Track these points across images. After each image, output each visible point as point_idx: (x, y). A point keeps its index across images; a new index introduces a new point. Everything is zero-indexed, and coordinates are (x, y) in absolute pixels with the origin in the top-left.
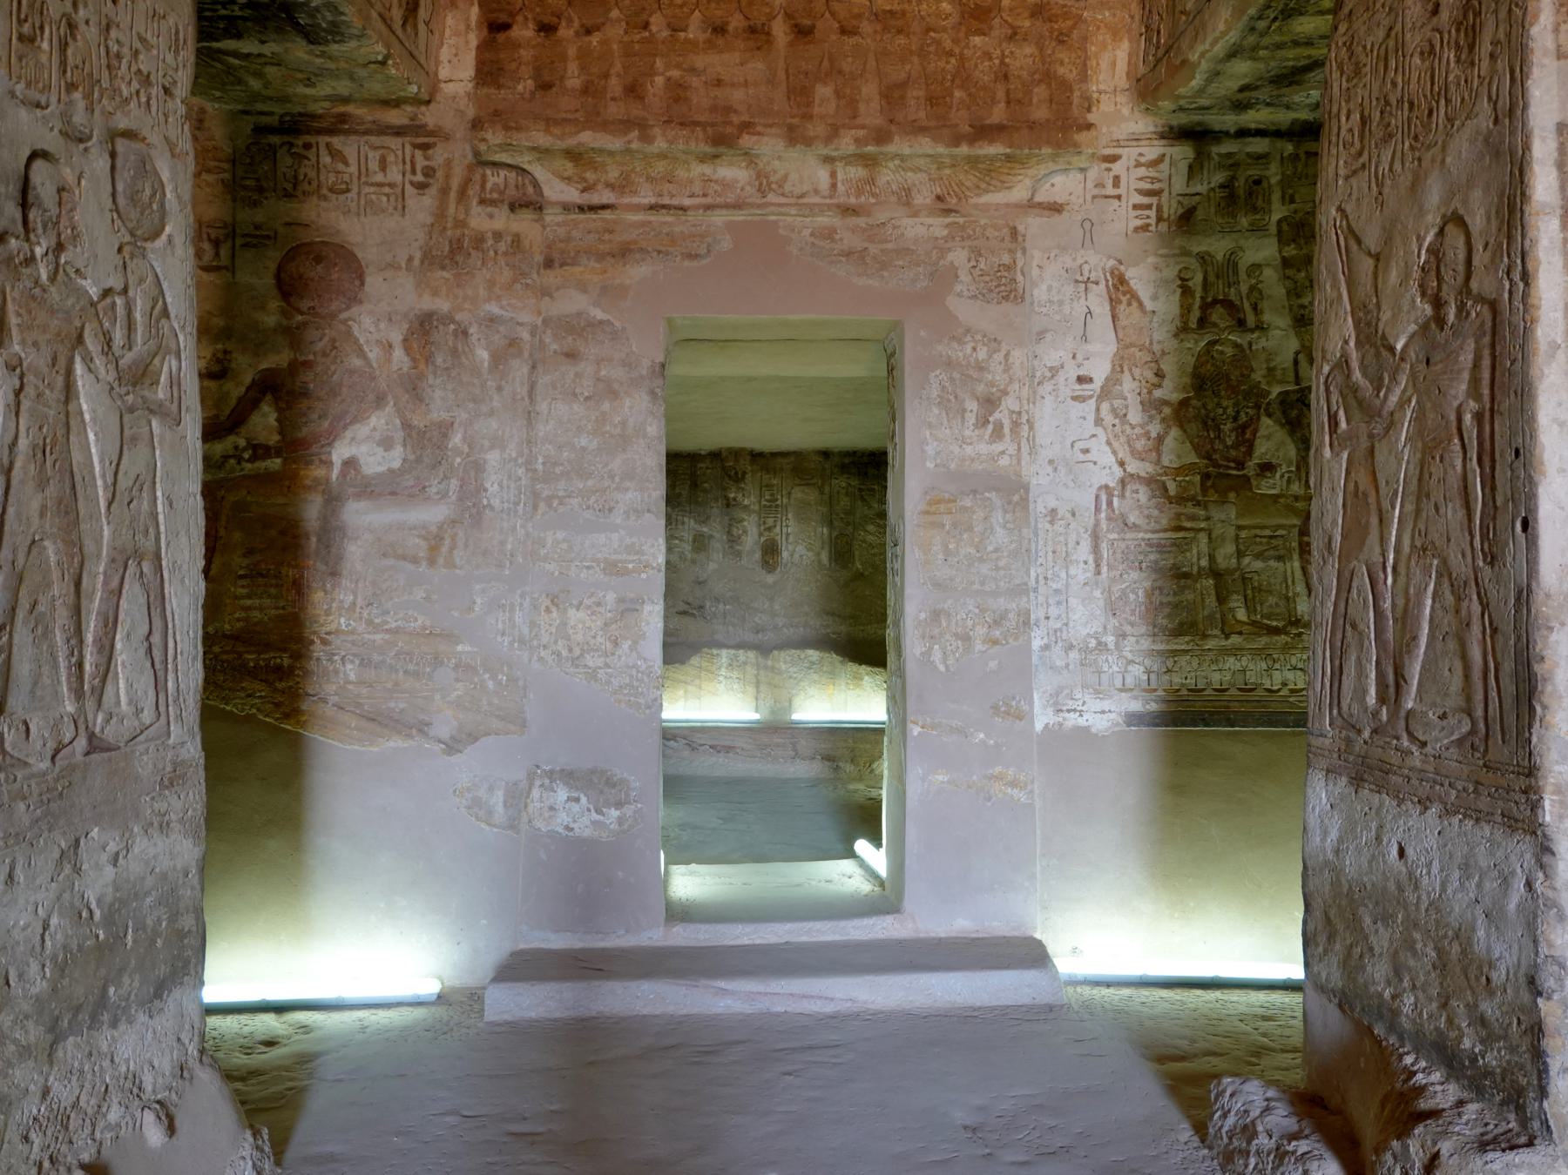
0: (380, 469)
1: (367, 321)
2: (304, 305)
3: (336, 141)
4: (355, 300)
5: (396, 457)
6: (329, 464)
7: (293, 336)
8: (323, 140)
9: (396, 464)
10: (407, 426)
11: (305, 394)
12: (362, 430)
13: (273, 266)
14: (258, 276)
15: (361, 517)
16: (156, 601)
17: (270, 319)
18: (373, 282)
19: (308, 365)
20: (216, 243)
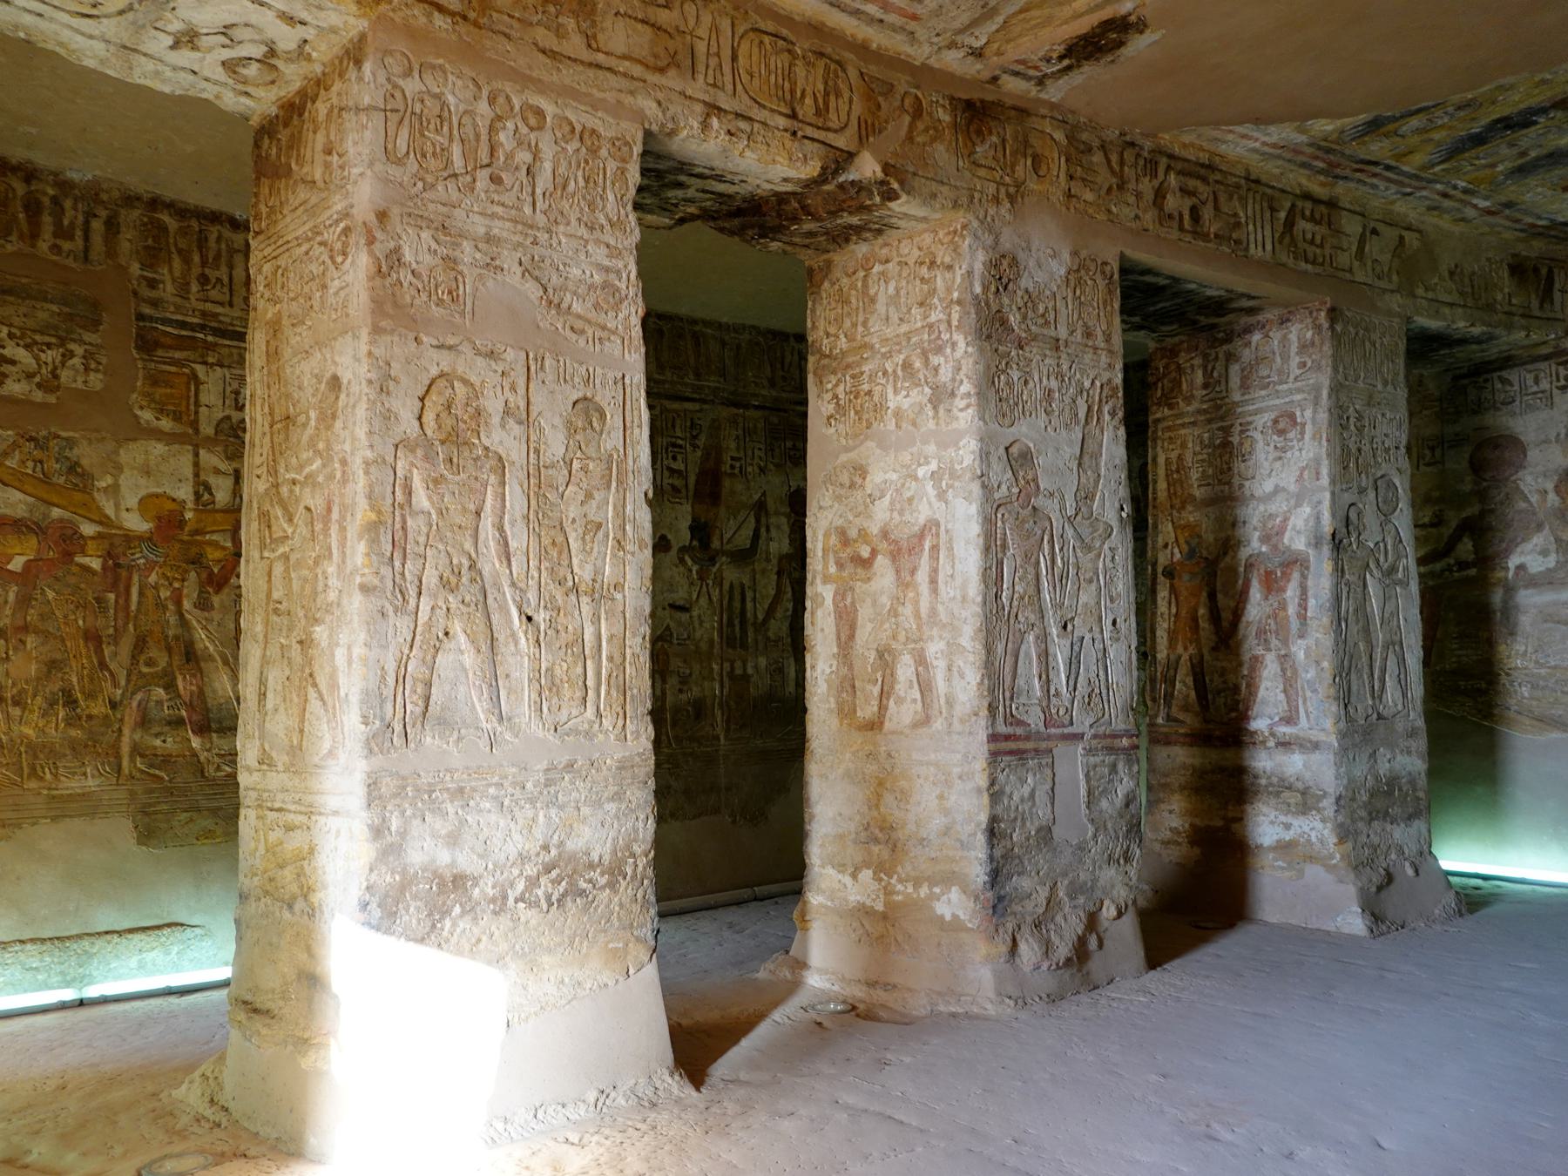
0: (1542, 569)
1: (1529, 479)
2: (1488, 475)
3: (1504, 374)
4: (1522, 467)
5: (1551, 561)
6: (1507, 569)
7: (1482, 495)
8: (1495, 375)
9: (1552, 565)
10: (1558, 540)
11: (1490, 528)
12: (1528, 546)
13: (1467, 456)
14: (1458, 462)
15: (1530, 601)
16: (1402, 661)
17: (1467, 487)
18: (1533, 455)
19: (1492, 511)
20: (1432, 449)
